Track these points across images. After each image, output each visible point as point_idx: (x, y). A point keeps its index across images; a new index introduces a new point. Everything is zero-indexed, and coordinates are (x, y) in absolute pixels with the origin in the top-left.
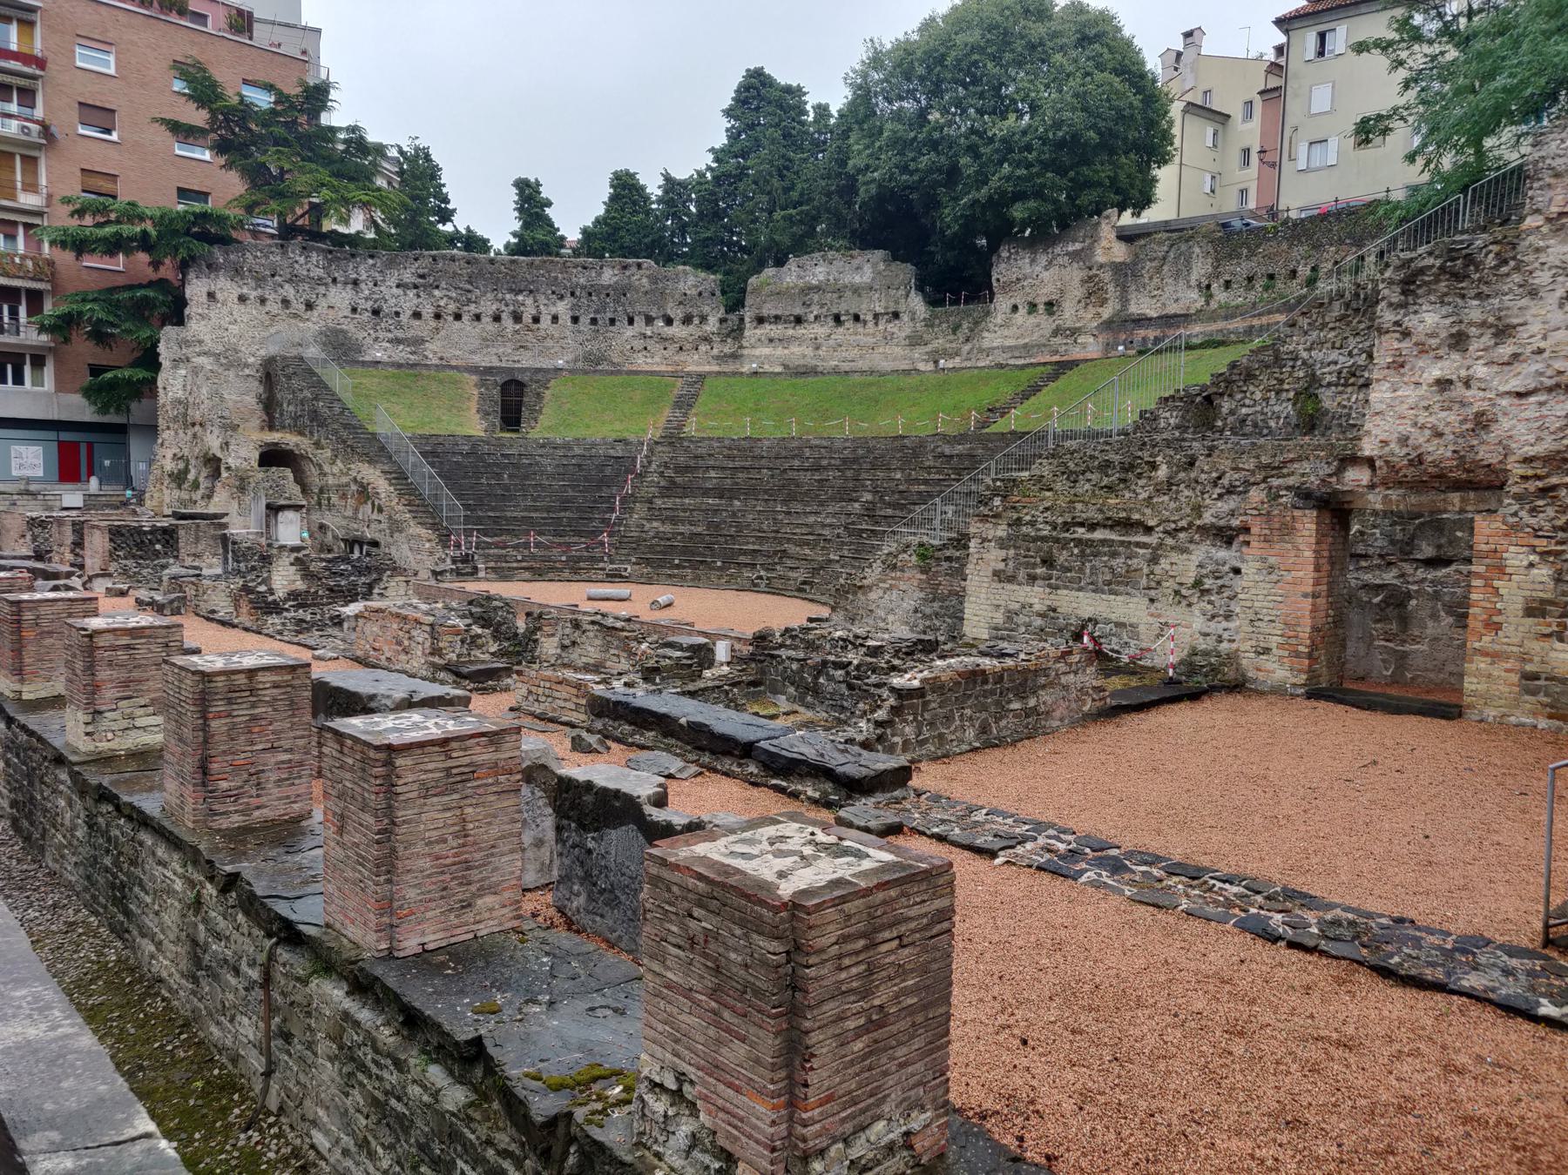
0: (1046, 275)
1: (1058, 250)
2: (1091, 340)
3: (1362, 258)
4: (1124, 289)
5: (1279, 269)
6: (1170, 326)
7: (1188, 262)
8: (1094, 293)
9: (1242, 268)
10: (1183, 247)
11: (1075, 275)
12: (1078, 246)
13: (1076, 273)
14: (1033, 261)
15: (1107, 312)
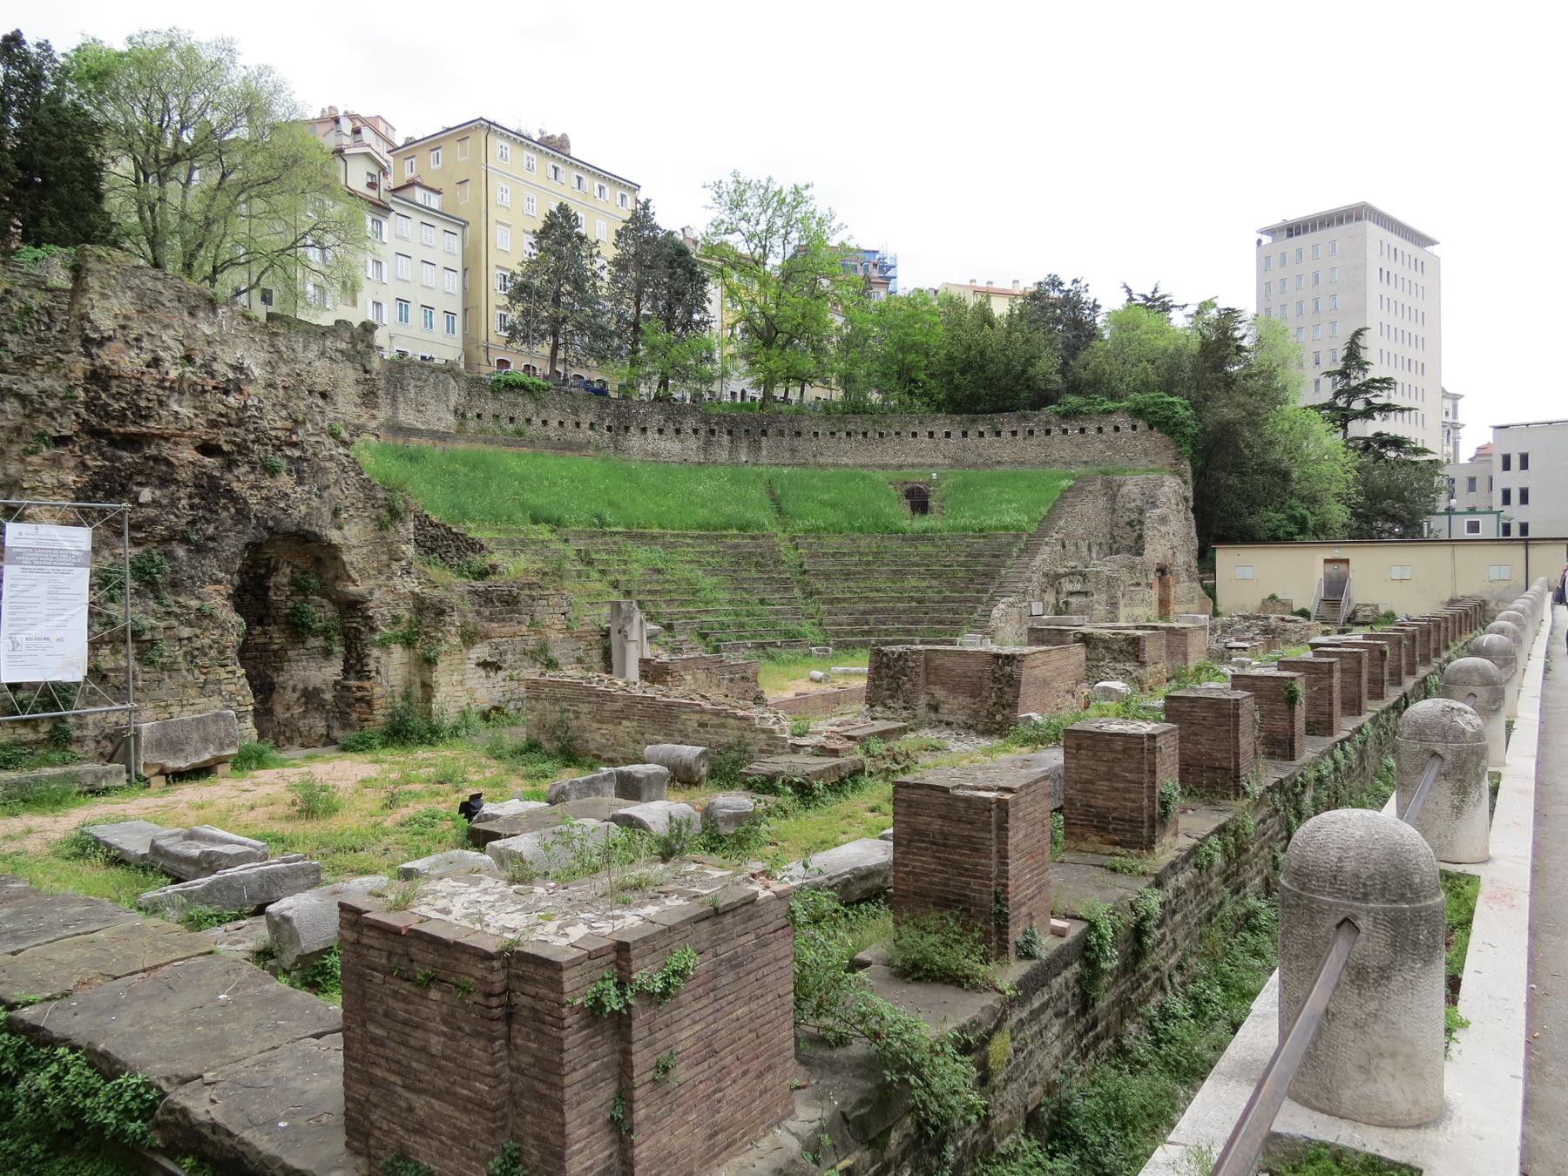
0: (317, 363)
1: (328, 343)
2: (373, 438)
3: (578, 425)
4: (394, 399)
5: (517, 413)
6: (440, 439)
7: (446, 392)
8: (369, 398)
9: (490, 407)
10: (441, 377)
11: (348, 375)
12: (344, 346)
13: (350, 372)
14: (305, 347)
15: (383, 414)
